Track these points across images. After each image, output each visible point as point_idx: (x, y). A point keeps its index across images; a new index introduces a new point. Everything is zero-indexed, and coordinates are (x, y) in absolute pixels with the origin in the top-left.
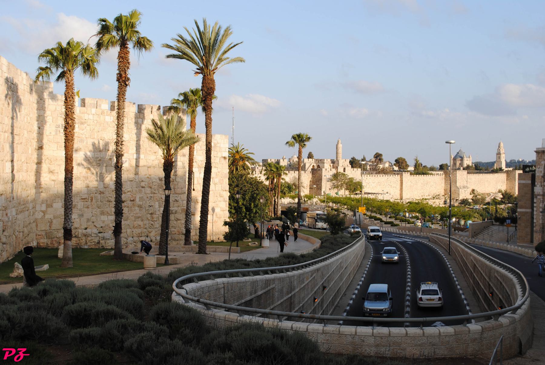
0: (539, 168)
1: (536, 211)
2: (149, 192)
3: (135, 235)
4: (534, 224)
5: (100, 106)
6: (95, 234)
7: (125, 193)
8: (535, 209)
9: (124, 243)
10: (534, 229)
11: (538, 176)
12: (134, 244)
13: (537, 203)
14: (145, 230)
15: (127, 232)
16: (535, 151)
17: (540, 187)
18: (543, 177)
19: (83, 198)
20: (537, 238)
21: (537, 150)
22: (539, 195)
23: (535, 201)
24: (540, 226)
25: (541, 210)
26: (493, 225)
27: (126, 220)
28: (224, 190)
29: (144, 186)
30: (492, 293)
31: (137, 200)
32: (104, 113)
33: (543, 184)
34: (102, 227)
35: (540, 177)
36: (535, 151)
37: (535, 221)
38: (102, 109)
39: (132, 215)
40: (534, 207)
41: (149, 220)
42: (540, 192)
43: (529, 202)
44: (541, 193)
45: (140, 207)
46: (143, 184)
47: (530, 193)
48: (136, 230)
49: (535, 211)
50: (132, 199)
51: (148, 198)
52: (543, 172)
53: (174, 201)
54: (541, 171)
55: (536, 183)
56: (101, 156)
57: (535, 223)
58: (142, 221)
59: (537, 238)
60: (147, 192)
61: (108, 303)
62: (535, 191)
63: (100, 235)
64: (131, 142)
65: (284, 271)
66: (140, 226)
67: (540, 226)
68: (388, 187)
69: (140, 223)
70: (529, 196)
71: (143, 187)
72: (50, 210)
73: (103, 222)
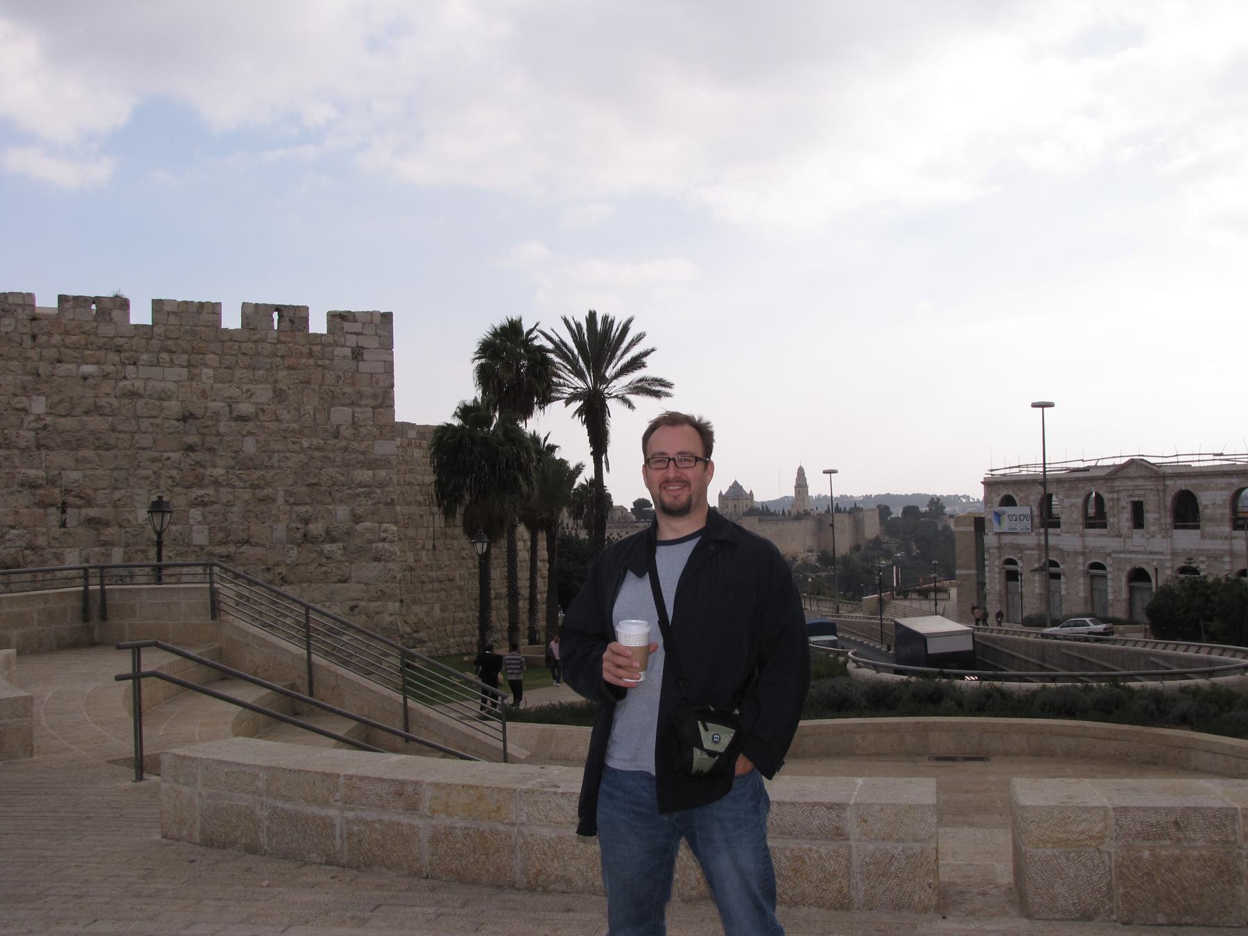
1: (989, 572)
2: (471, 566)
3: (458, 634)
5: (407, 434)
6: (409, 634)
8: (986, 569)
11: (989, 519)
14: (469, 626)
15: (446, 630)
16: (982, 483)
22: (993, 548)
23: (986, 556)
26: (894, 599)
29: (465, 556)
32: (412, 445)
34: (415, 623)
36: (982, 483)
38: (408, 438)
39: (451, 602)
41: (472, 610)
46: (464, 554)
48: (458, 626)
50: (451, 578)
55: (986, 531)
56: (410, 512)
58: (464, 611)
63: (415, 635)
66: (462, 619)
69: (461, 615)
71: (463, 558)
73: (416, 615)
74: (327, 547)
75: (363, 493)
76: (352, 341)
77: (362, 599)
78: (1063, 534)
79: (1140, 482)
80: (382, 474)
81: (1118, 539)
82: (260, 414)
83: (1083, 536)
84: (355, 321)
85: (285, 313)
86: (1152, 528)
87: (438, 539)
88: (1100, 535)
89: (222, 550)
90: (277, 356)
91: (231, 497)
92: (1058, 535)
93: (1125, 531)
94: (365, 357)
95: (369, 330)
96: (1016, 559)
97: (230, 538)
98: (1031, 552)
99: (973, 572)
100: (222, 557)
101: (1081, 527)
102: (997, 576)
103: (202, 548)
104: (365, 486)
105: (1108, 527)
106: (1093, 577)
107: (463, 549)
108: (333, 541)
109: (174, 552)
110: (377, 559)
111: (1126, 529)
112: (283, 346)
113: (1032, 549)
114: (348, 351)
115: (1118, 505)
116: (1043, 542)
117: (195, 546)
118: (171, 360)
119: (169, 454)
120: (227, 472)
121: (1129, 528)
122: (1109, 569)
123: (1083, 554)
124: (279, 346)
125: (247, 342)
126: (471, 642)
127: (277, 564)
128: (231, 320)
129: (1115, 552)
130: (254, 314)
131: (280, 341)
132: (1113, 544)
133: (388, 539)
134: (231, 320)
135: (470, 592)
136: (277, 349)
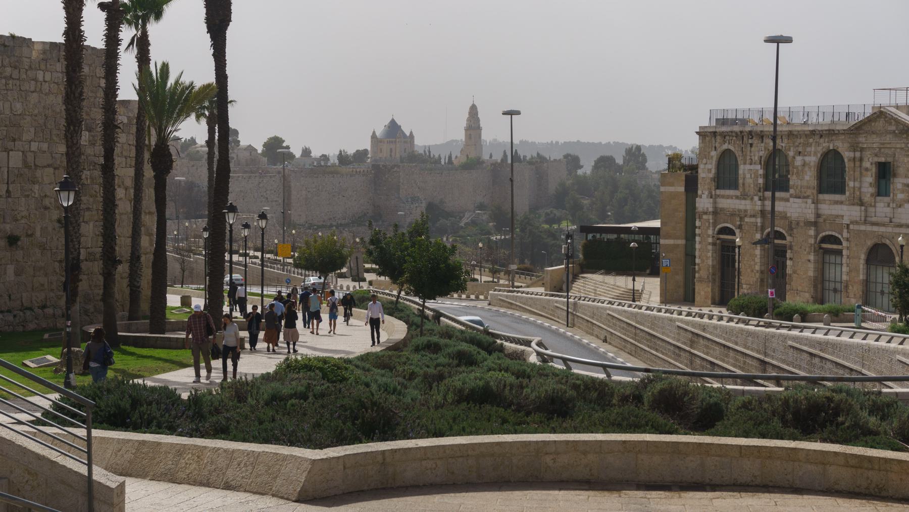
0: (706, 164)
7: (17, 220)
8: (698, 239)
9: (21, 320)
10: (697, 275)
11: (703, 178)
12: (36, 321)
13: (702, 228)
14: (52, 294)
16: (697, 133)
17: (707, 198)
18: (713, 179)
20: (702, 293)
21: (702, 130)
22: (706, 213)
23: (698, 223)
24: (708, 270)
25: (710, 240)
27: (19, 275)
28: (147, 211)
29: (49, 205)
31: (38, 234)
33: (713, 193)
35: (708, 181)
36: (697, 133)
39: (29, 263)
40: (694, 235)
41: (57, 274)
42: (707, 208)
44: (711, 209)
45: (43, 247)
49: (697, 242)
50: (30, 232)
51: (54, 229)
52: (713, 171)
53: (98, 235)
54: (711, 169)
55: (699, 192)
57: (699, 264)
58: (46, 275)
59: (702, 293)
61: (655, 362)
62: (697, 205)
64: (25, 117)
66: (43, 285)
67: (708, 270)
68: (261, 202)
71: (46, 208)
78: (792, 200)
79: (888, 138)
81: (858, 208)
83: (816, 202)
86: (900, 196)
87: (13, 182)
93: (867, 198)
96: (734, 228)
98: (753, 220)
99: (682, 242)
101: (815, 192)
102: (710, 247)
105: (847, 193)
107: (46, 196)
111: (869, 195)
113: (754, 216)
115: (861, 166)
116: (769, 208)
121: (872, 195)
122: (845, 244)
123: (815, 224)
126: (54, 315)
129: (852, 222)
132: (849, 213)
135: (55, 251)
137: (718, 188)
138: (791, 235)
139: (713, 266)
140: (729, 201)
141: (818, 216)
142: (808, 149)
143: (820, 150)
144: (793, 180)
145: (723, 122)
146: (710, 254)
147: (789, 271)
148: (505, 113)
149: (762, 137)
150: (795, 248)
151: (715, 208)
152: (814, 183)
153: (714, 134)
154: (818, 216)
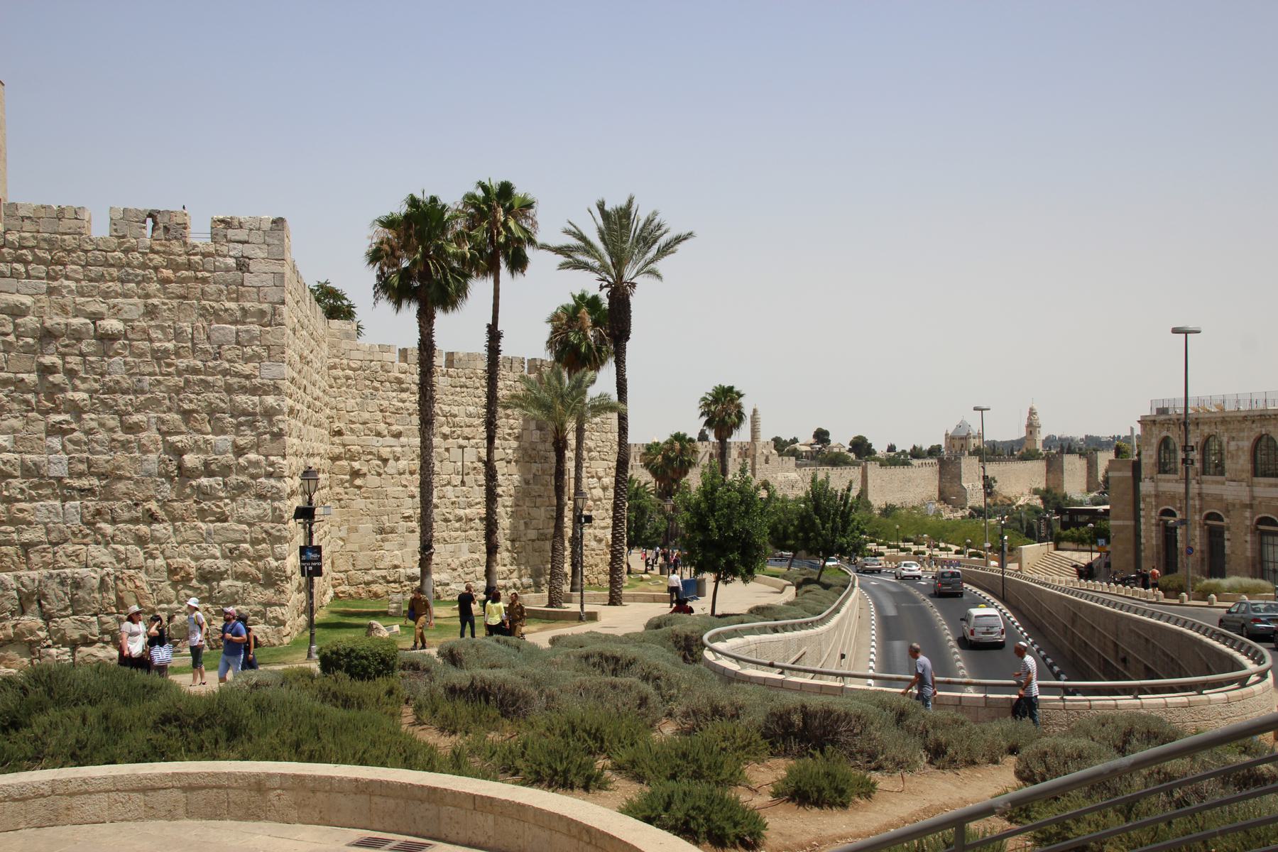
4: (1142, 547)
8: (1142, 520)
18: (1155, 465)
19: (406, 515)
22: (1149, 496)
23: (1142, 506)
25: (1153, 521)
30: (1124, 660)
37: (1143, 540)
43: (1130, 508)
44: (1153, 493)
47: (1130, 492)
60: (507, 504)
65: (779, 629)
70: (1129, 497)
72: (354, 536)
74: (204, 481)
75: (246, 421)
76: (237, 250)
77: (245, 541)
80: (270, 400)
82: (129, 332)
83: (1251, 485)
84: (241, 227)
85: (159, 219)
87: (468, 474)
88: (1271, 485)
89: (84, 483)
90: (150, 268)
91: (94, 424)
92: (1224, 484)
94: (251, 269)
95: (256, 237)
97: (92, 469)
99: (1131, 523)
100: (83, 491)
101: (1249, 475)
102: (1154, 528)
103: (60, 479)
104: (249, 414)
106: (1263, 533)
108: (211, 474)
109: (27, 484)
110: (261, 497)
112: (156, 256)
114: (231, 262)
117: (51, 478)
118: (27, 271)
119: (20, 376)
120: (91, 397)
123: (1251, 506)
124: (151, 256)
125: (114, 251)
127: (147, 500)
128: (100, 229)
130: (125, 220)
131: (153, 251)
133: (274, 475)
134: (100, 229)
136: (149, 259)
137: (1159, 472)
138: (1227, 517)
139: (1157, 545)
140: (1170, 484)
141: (1253, 498)
142: (1242, 434)
143: (1254, 435)
144: (1228, 464)
145: (1163, 411)
146: (1153, 535)
147: (1227, 551)
148: (975, 409)
149: (1198, 424)
150: (1232, 529)
151: (1157, 490)
152: (1249, 466)
153: (1154, 422)
154: (1253, 498)
